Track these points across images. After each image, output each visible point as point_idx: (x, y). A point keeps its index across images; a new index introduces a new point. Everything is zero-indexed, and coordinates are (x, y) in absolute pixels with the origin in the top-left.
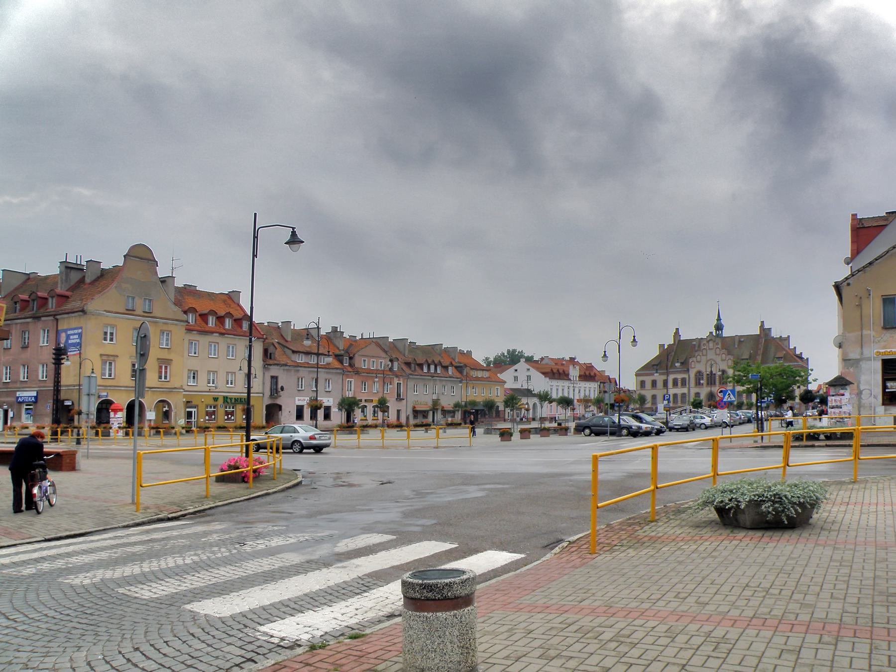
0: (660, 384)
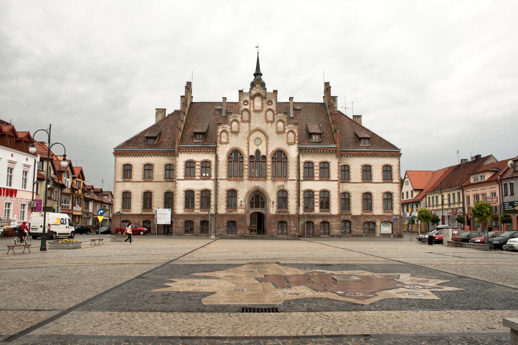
0: (159, 172)
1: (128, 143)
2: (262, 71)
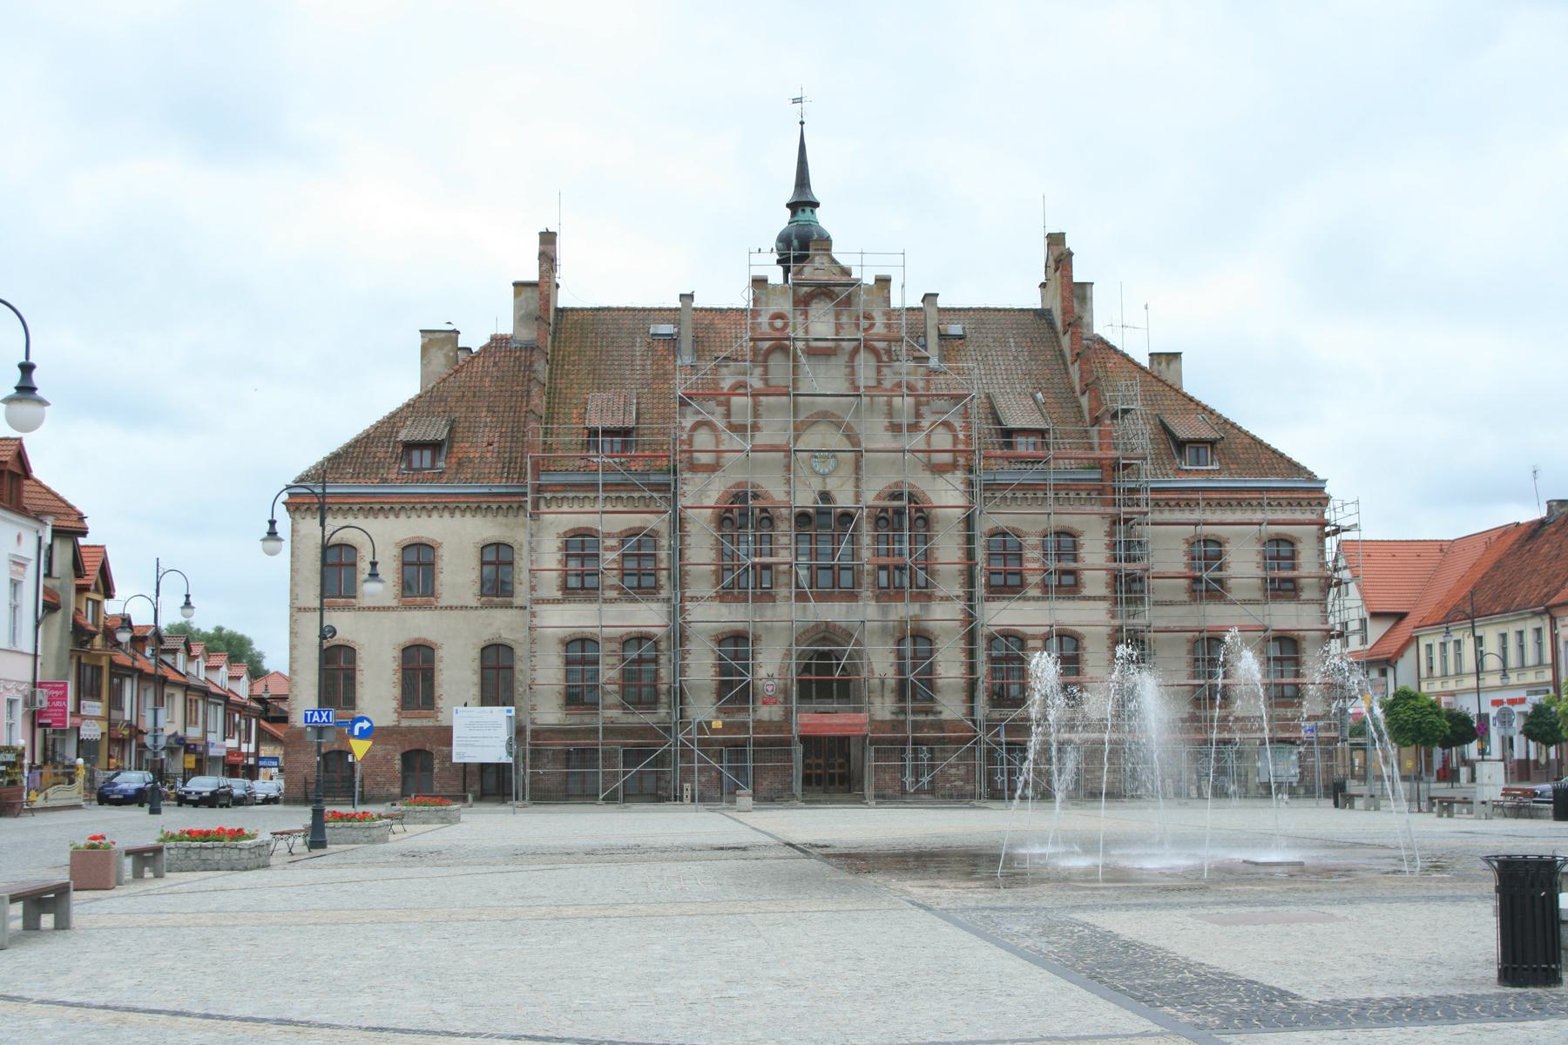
0: (458, 574)
1: (337, 463)
2: (817, 190)
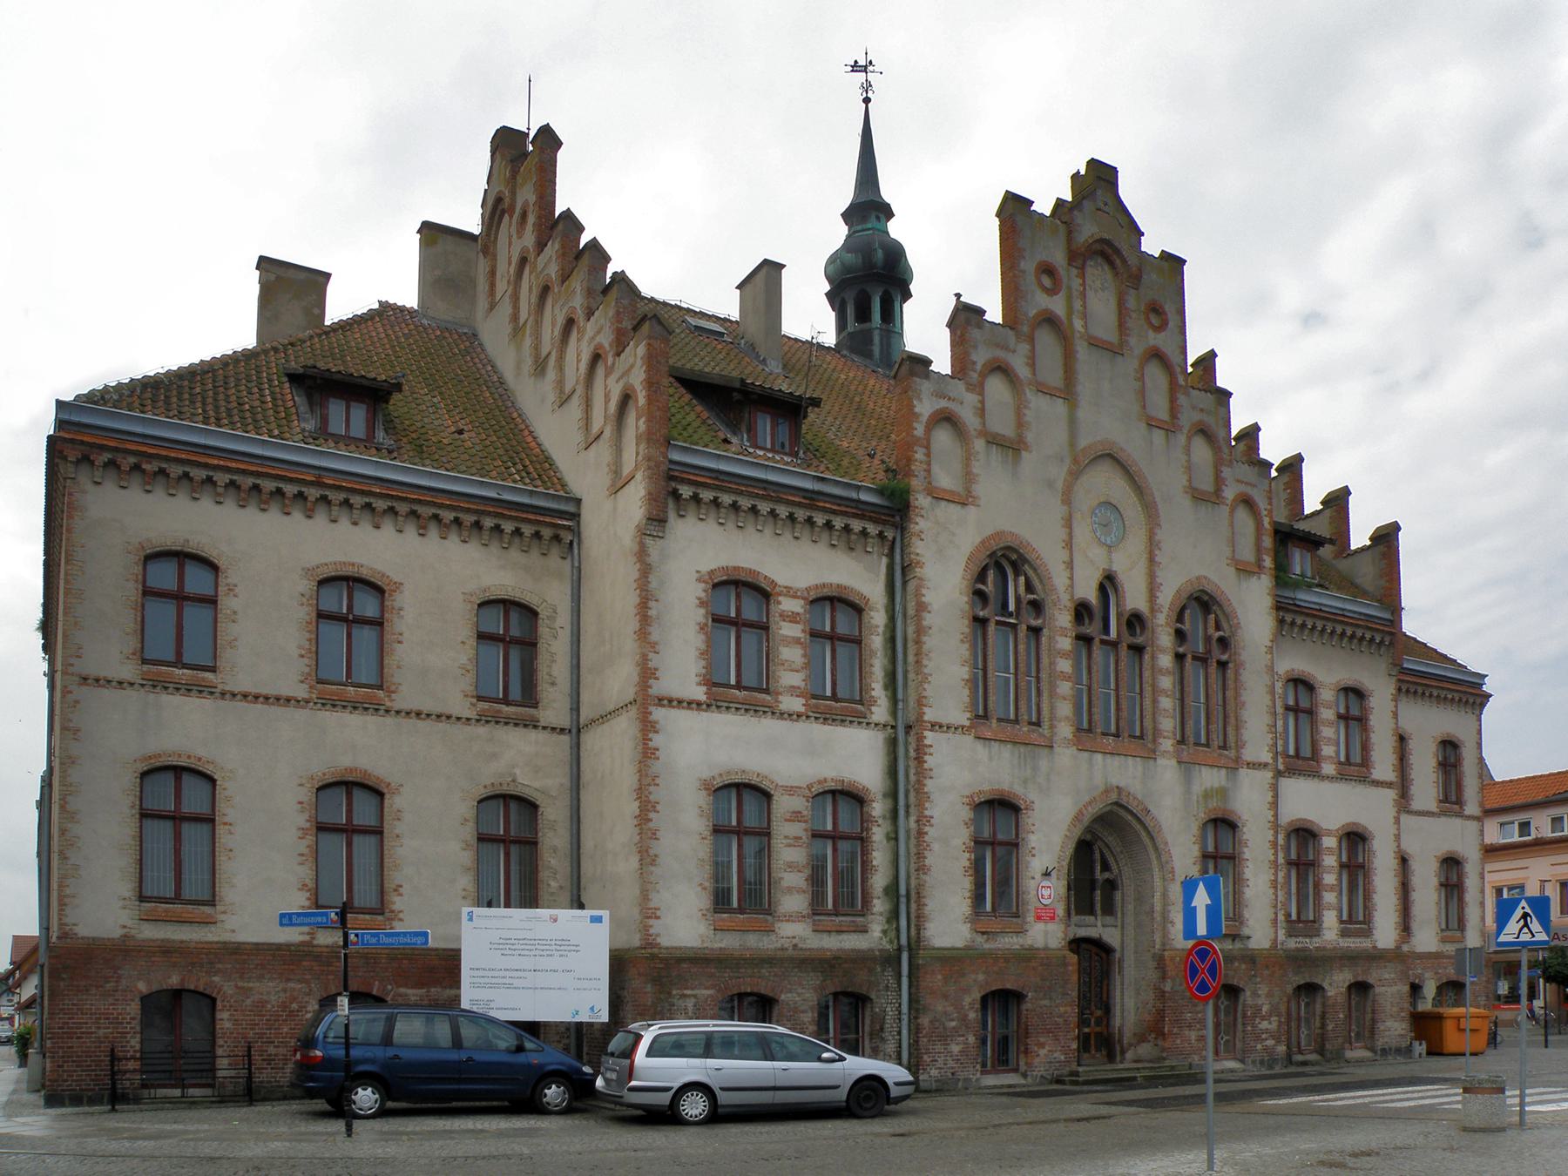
0: (433, 645)
